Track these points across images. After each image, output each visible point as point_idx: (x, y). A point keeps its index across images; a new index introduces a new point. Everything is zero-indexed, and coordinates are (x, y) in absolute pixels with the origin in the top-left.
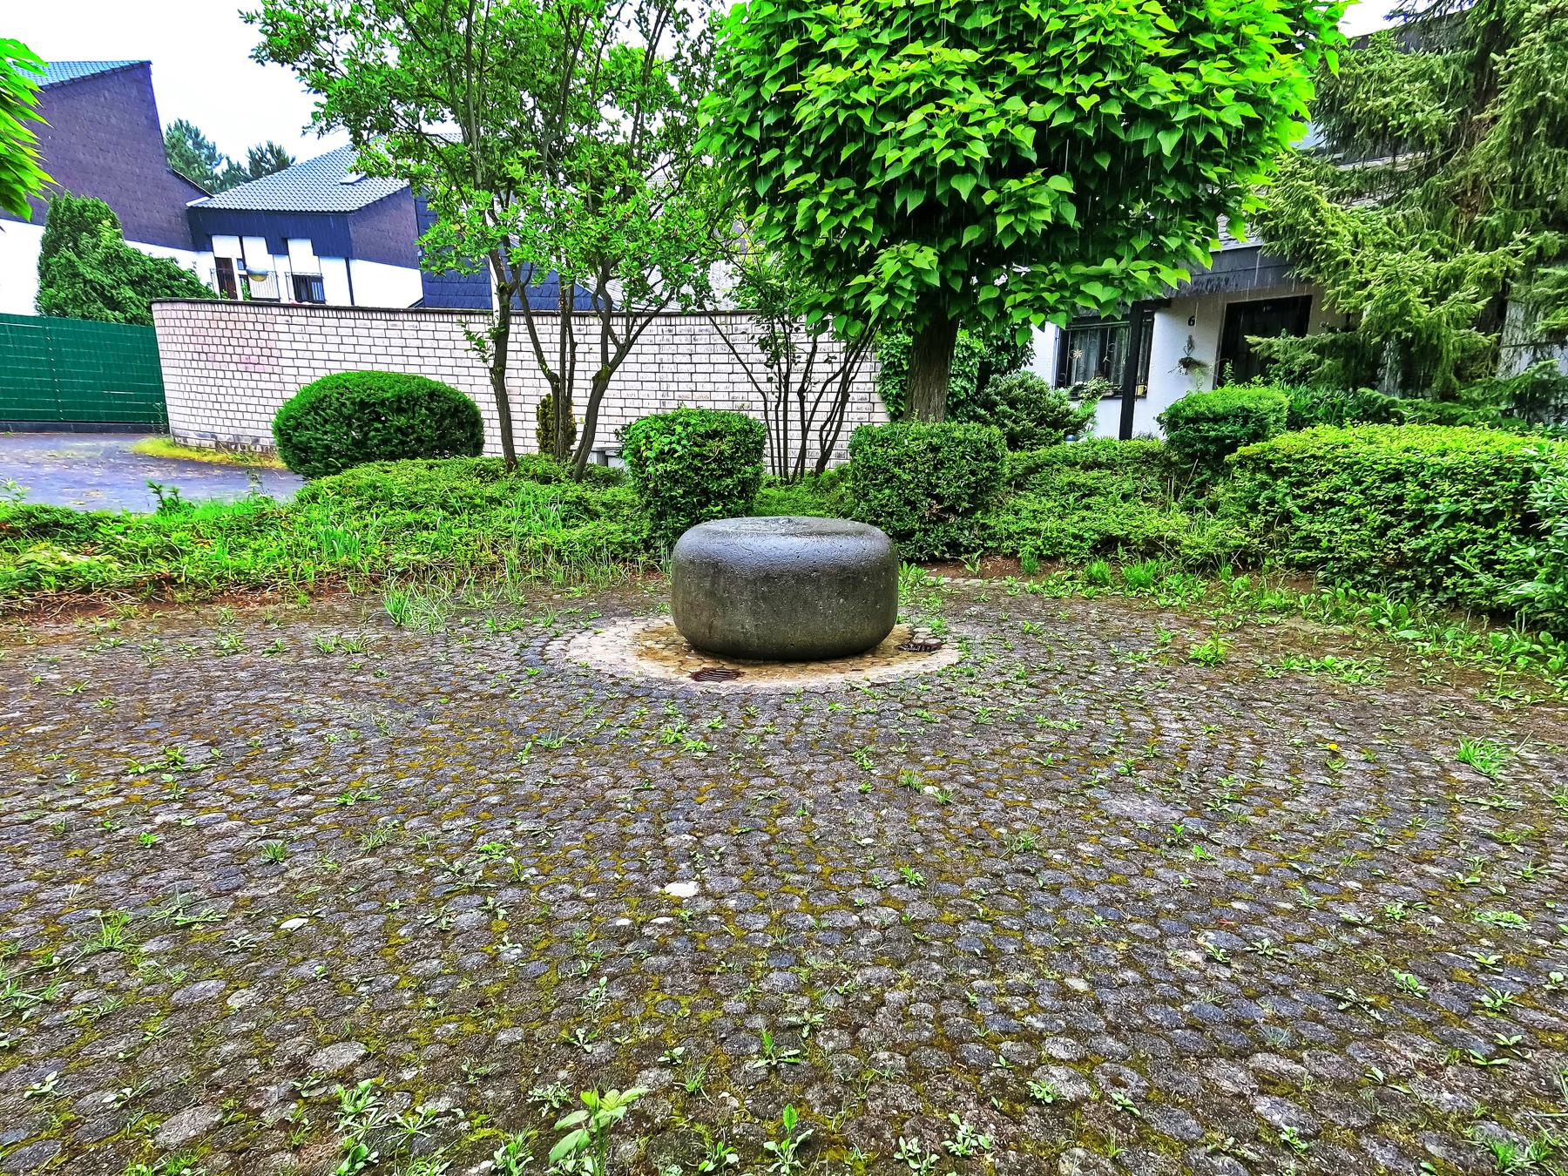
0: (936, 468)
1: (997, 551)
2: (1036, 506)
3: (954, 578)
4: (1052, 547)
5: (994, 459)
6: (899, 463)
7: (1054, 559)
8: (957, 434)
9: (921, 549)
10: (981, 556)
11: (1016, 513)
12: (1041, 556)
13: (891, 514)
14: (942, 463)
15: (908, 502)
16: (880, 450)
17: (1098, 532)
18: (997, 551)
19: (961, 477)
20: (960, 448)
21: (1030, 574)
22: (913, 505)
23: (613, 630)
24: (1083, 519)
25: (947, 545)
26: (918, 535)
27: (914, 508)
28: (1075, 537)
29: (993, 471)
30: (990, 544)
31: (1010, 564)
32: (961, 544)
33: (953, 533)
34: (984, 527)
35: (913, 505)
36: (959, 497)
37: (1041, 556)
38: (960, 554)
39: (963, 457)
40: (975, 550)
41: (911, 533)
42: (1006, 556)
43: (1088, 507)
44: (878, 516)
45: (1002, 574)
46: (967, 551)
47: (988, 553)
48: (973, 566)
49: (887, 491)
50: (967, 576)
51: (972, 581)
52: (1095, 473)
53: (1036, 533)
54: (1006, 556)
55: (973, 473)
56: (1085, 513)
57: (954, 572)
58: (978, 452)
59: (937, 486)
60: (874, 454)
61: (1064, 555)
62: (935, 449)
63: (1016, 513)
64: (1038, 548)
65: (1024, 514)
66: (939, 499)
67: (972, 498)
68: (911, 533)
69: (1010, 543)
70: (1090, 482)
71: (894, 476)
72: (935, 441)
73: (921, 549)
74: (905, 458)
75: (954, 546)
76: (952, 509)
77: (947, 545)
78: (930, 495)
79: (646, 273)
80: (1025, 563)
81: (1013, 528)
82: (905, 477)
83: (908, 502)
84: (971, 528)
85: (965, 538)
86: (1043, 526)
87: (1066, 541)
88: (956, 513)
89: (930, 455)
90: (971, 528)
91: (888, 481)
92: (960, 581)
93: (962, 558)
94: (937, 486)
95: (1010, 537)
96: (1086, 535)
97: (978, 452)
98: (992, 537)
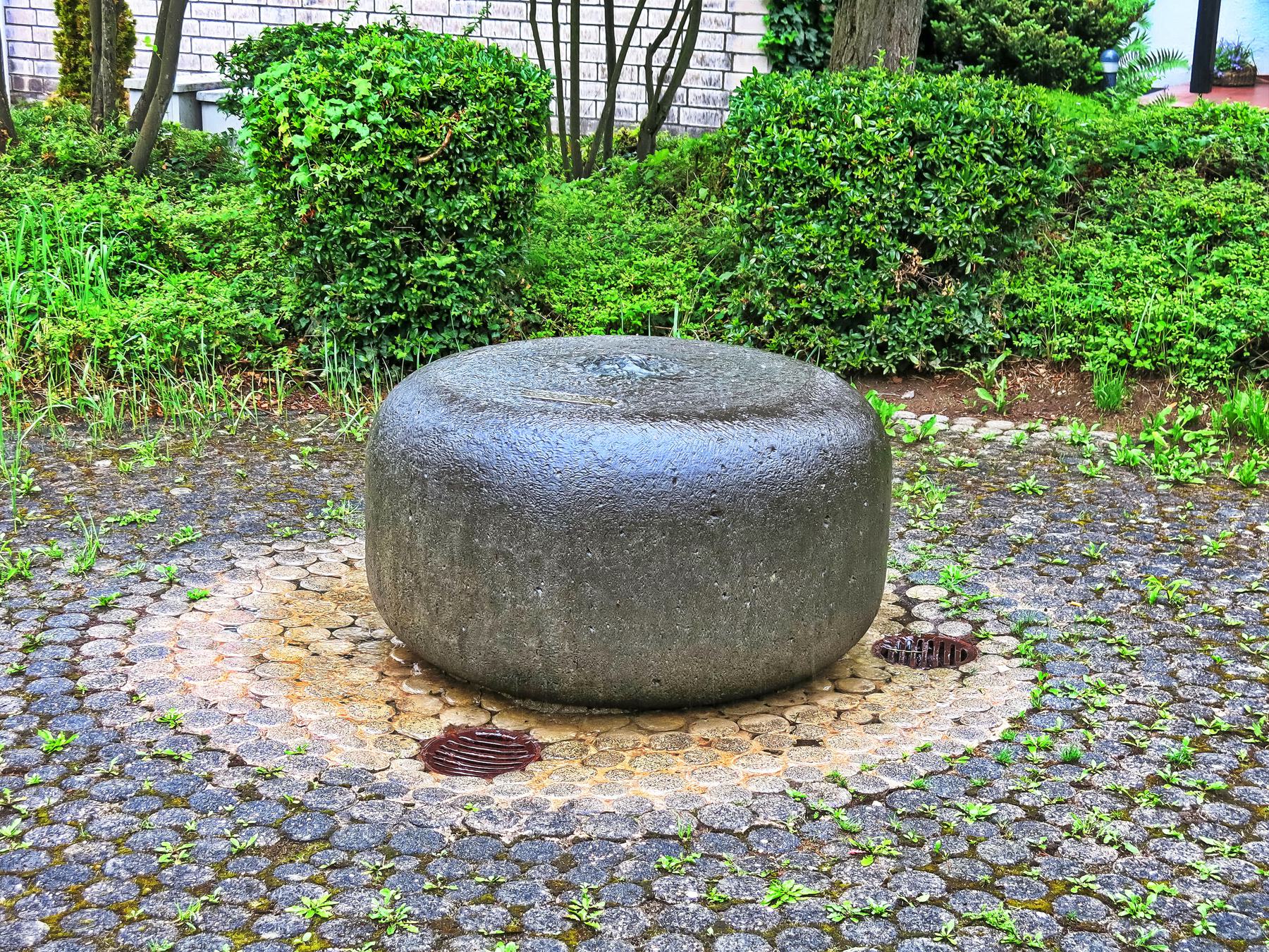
0: (919, 178)
1: (1038, 355)
2: (1117, 261)
3: (952, 414)
4: (1154, 350)
5: (1041, 161)
6: (841, 166)
7: (1156, 375)
8: (966, 106)
9: (882, 349)
10: (1005, 365)
11: (1079, 275)
12: (1131, 371)
13: (822, 276)
14: (932, 168)
15: (860, 251)
16: (800, 136)
17: (1247, 325)
18: (1038, 355)
19: (973, 199)
20: (973, 139)
21: (1109, 412)
22: (871, 259)
23: (231, 587)
24: (1216, 294)
25: (938, 342)
26: (878, 322)
27: (872, 265)
28: (1204, 333)
29: (1036, 187)
30: (1024, 339)
31: (1063, 387)
32: (964, 341)
33: (952, 316)
34: (1013, 302)
35: (871, 259)
36: (965, 243)
37: (1131, 371)
38: (963, 360)
39: (979, 158)
40: (993, 353)
41: (864, 317)
42: (1055, 367)
43: (1223, 268)
44: (793, 278)
45: (1053, 409)
46: (976, 353)
47: (1019, 360)
48: (991, 388)
49: (814, 227)
50: (984, 413)
51: (994, 427)
52: (1226, 187)
53: (1125, 322)
54: (1055, 367)
55: (997, 191)
56: (1216, 280)
57: (946, 400)
58: (1008, 145)
59: (921, 217)
60: (787, 144)
61: (1175, 368)
62: (918, 138)
63: (1079, 275)
64: (1124, 354)
65: (1095, 277)
66: (927, 247)
67: (995, 247)
68: (864, 317)
69: (1068, 340)
70: (1223, 210)
71: (830, 194)
72: (920, 121)
73: (882, 349)
74: (857, 157)
75: (949, 342)
76: (950, 267)
77: (938, 342)
78: (903, 236)
79: (351, 32)
80: (1099, 388)
81: (1073, 308)
82: (856, 197)
83: (860, 251)
84: (986, 306)
85: (977, 327)
86: (1134, 306)
87: (1184, 343)
88: (959, 275)
89: (909, 152)
90: (986, 306)
91: (815, 203)
92: (965, 424)
93: (967, 370)
94: (921, 217)
95: (1066, 327)
96: (1224, 331)
97: (1008, 145)
98: (1030, 325)
